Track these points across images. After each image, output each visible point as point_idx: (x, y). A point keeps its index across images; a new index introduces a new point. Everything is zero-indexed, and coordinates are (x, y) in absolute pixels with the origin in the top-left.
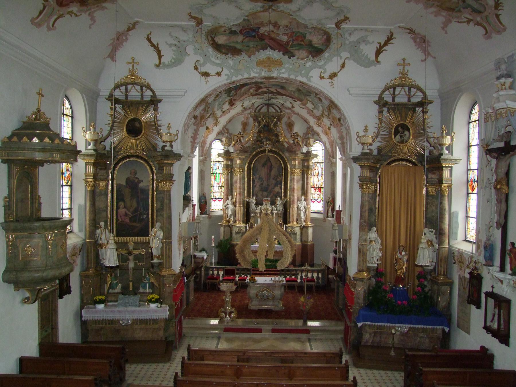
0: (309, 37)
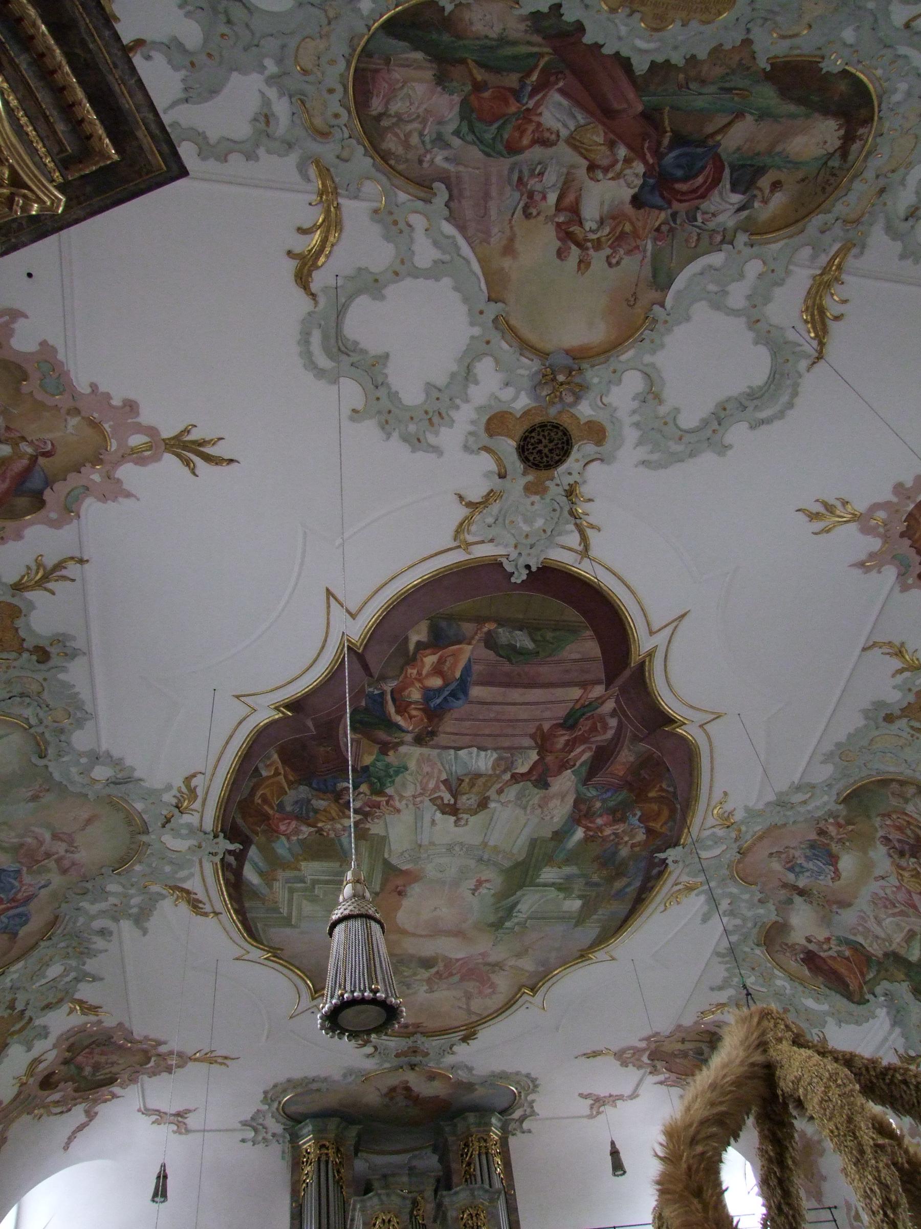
0: (446, 106)
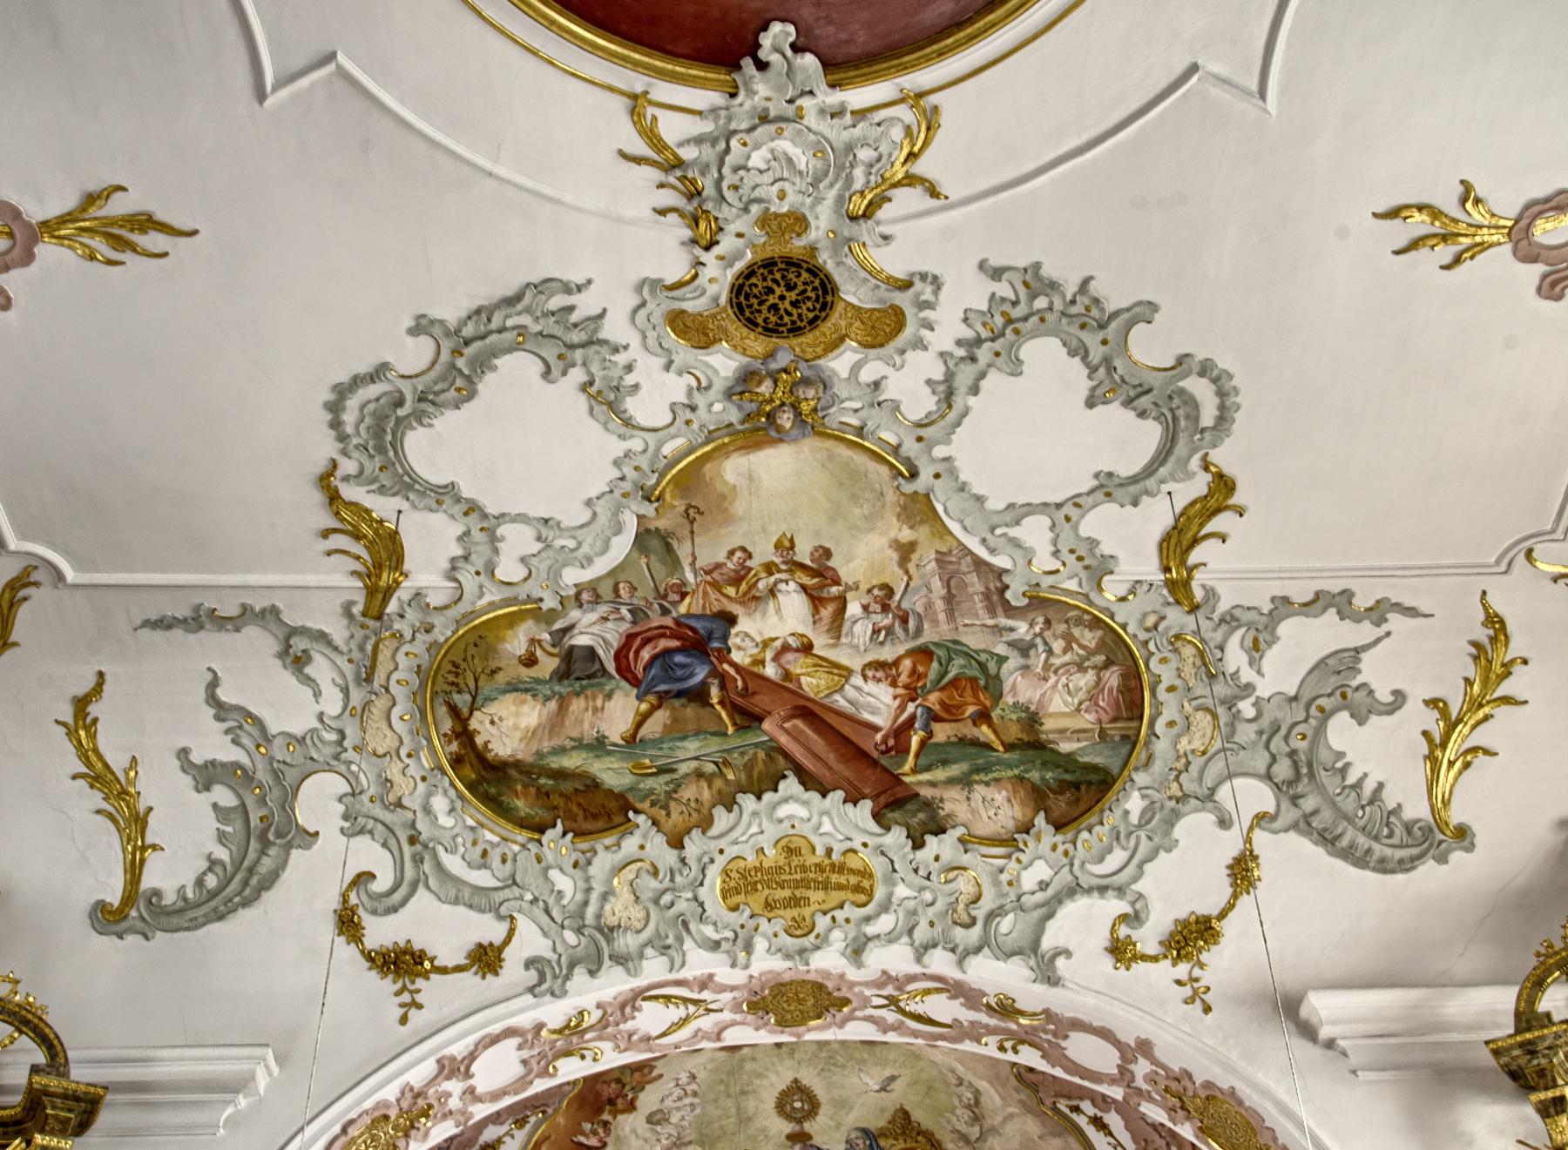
0: (1020, 688)
